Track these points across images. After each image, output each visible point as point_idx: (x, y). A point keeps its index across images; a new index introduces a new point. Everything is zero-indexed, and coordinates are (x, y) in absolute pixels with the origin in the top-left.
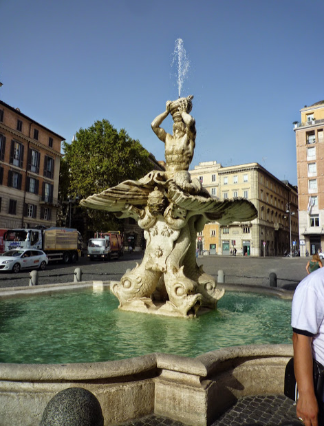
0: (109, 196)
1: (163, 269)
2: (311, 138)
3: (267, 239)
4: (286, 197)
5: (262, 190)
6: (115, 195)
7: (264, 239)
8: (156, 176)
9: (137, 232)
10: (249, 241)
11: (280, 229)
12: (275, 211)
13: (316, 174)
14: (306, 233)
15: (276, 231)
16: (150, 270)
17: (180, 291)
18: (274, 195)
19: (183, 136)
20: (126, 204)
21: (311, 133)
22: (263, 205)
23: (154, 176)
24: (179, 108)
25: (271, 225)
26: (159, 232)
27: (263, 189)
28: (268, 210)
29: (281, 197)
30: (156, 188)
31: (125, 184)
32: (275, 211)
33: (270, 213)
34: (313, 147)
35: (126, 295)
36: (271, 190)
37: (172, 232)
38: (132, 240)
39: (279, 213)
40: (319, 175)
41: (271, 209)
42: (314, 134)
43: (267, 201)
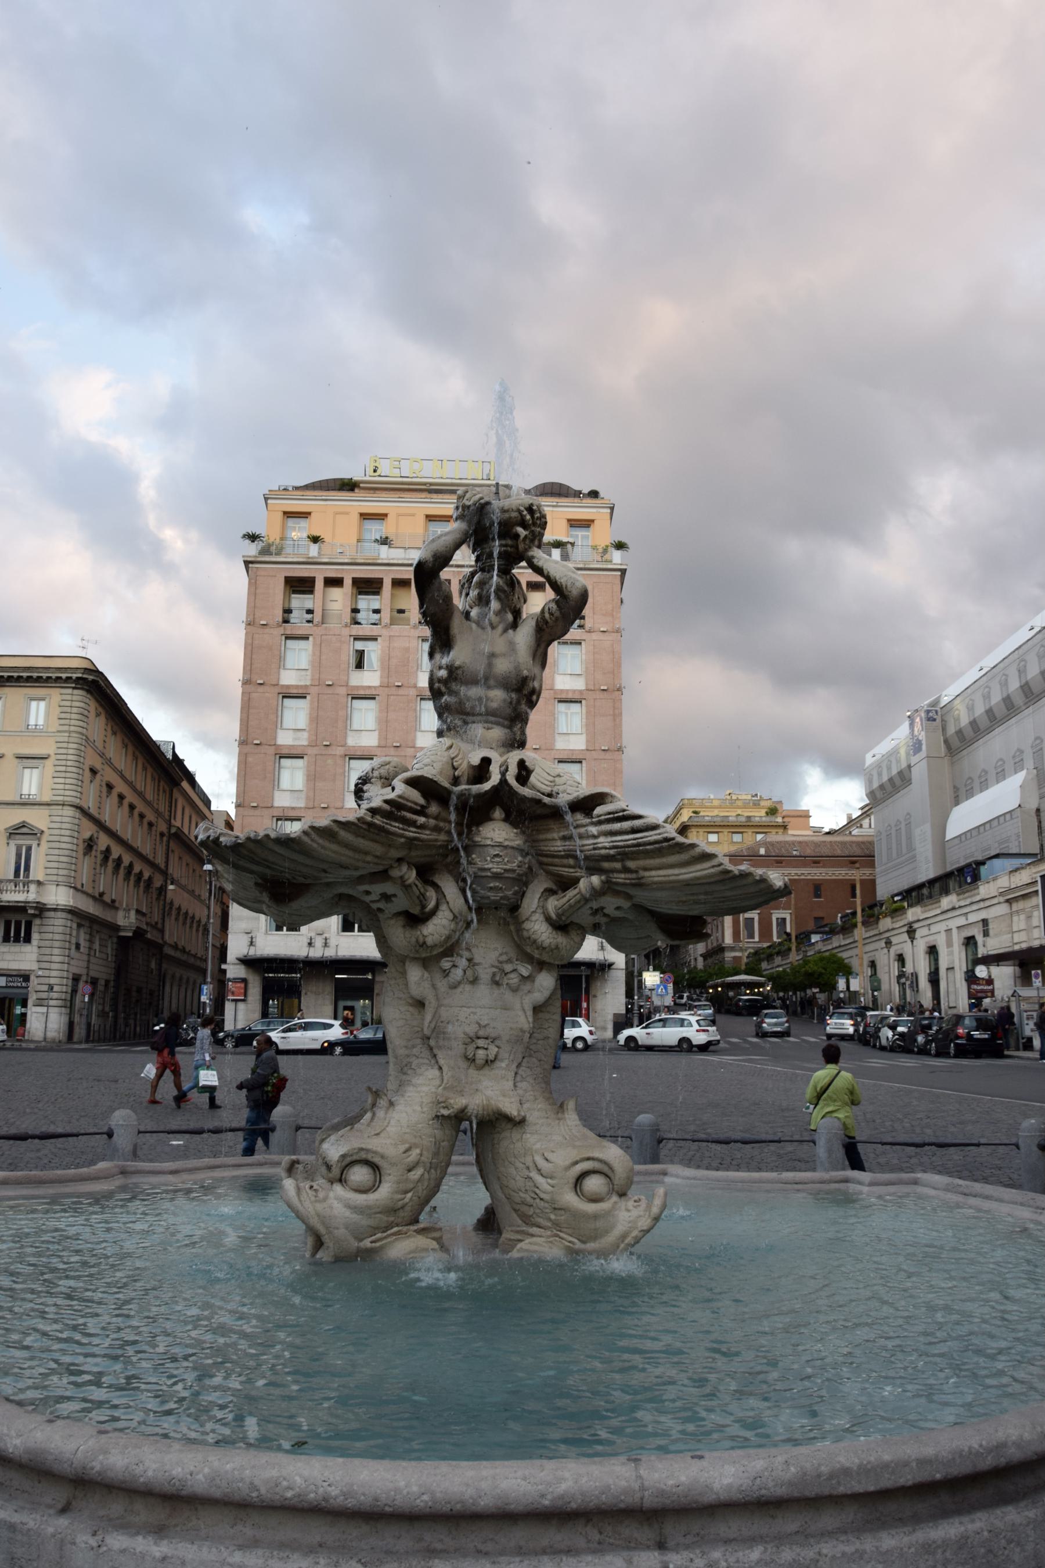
0: (381, 829)
2: (299, 602)
3: (92, 974)
4: (163, 807)
5: (93, 771)
6: (395, 827)
7: (84, 972)
10: (26, 978)
11: (139, 933)
12: (127, 859)
13: (303, 739)
14: (253, 952)
15: (124, 942)
17: (594, 1184)
18: (130, 797)
20: (400, 860)
21: (300, 585)
22: (89, 830)
25: (107, 916)
26: (485, 974)
27: (98, 766)
28: (107, 852)
29: (148, 803)
30: (498, 813)
32: (127, 859)
33: (110, 864)
34: (305, 638)
35: (365, 1222)
36: (122, 777)
37: (530, 978)
39: (137, 869)
40: (312, 745)
41: (116, 851)
42: (311, 591)
43: (106, 818)
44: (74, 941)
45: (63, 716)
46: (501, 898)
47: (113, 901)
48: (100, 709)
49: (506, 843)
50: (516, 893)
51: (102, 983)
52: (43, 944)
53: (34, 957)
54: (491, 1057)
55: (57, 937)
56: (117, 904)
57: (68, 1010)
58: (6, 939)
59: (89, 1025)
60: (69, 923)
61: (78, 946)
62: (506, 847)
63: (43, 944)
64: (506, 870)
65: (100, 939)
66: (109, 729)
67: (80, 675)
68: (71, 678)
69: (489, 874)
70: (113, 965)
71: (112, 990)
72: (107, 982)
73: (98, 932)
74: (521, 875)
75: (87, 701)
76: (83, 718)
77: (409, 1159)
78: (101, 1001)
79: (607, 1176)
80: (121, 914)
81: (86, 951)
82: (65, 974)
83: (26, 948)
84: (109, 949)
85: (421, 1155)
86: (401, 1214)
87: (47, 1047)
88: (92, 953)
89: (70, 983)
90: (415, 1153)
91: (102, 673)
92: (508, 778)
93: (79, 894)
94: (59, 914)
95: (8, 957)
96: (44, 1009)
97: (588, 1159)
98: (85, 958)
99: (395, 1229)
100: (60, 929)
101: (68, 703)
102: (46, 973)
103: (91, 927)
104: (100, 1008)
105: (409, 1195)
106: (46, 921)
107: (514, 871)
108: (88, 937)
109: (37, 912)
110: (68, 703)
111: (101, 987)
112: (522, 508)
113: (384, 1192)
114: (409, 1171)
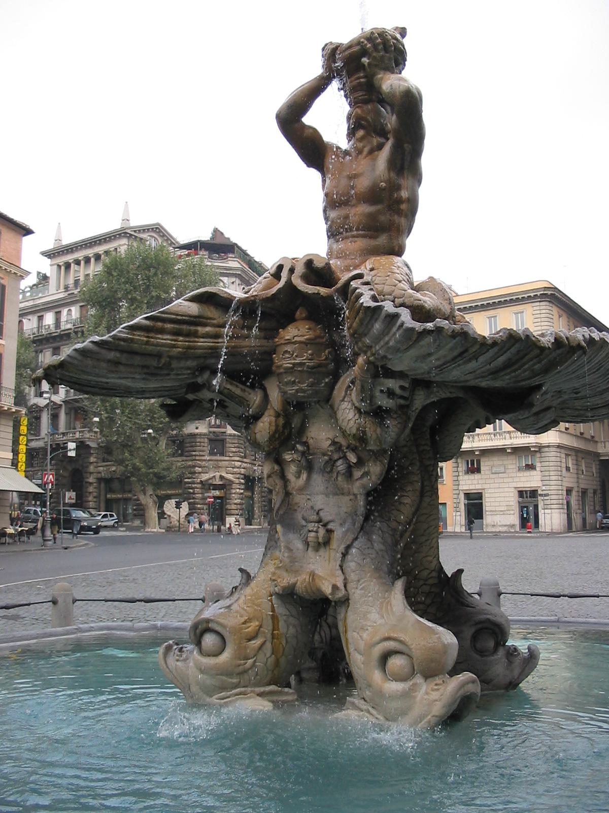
1: (335, 588)
3: (582, 486)
8: (300, 269)
9: (230, 477)
16: (289, 595)
17: (396, 662)
19: (380, 147)
23: (292, 271)
24: (365, 60)
25: (590, 447)
31: (192, 299)
38: (215, 498)
44: (564, 465)
45: (536, 320)
46: (297, 391)
47: (593, 437)
48: (561, 312)
49: (296, 339)
50: (312, 385)
51: (592, 491)
52: (543, 469)
53: (539, 478)
54: (321, 540)
55: (551, 464)
56: (596, 439)
57: (566, 511)
58: (520, 469)
59: (584, 520)
60: (558, 454)
61: (568, 469)
62: (295, 343)
63: (543, 469)
64: (294, 364)
65: (585, 463)
66: (571, 324)
67: (542, 292)
68: (537, 295)
69: (282, 370)
70: (598, 479)
71: (600, 496)
72: (595, 492)
73: (583, 458)
74: (313, 368)
75: (550, 308)
76: (549, 320)
77: (249, 629)
78: (592, 504)
79: (408, 655)
80: (599, 445)
81: (575, 471)
82: (560, 488)
83: (533, 473)
84: (594, 468)
85: (261, 626)
86: (246, 677)
87: (551, 534)
88: (580, 472)
89: (565, 493)
90: (254, 624)
91: (557, 289)
92: (292, 278)
93: (564, 435)
94: (552, 449)
95: (523, 479)
96: (549, 511)
97: (388, 639)
98: (575, 476)
99: (238, 690)
100: (553, 459)
101: (538, 312)
102: (548, 488)
103: (576, 456)
104: (592, 508)
105: (250, 661)
106: (543, 455)
107: (304, 364)
108: (575, 462)
109: (537, 449)
110: (538, 312)
111: (590, 494)
112: (362, 40)
113: (225, 656)
114: (250, 640)
